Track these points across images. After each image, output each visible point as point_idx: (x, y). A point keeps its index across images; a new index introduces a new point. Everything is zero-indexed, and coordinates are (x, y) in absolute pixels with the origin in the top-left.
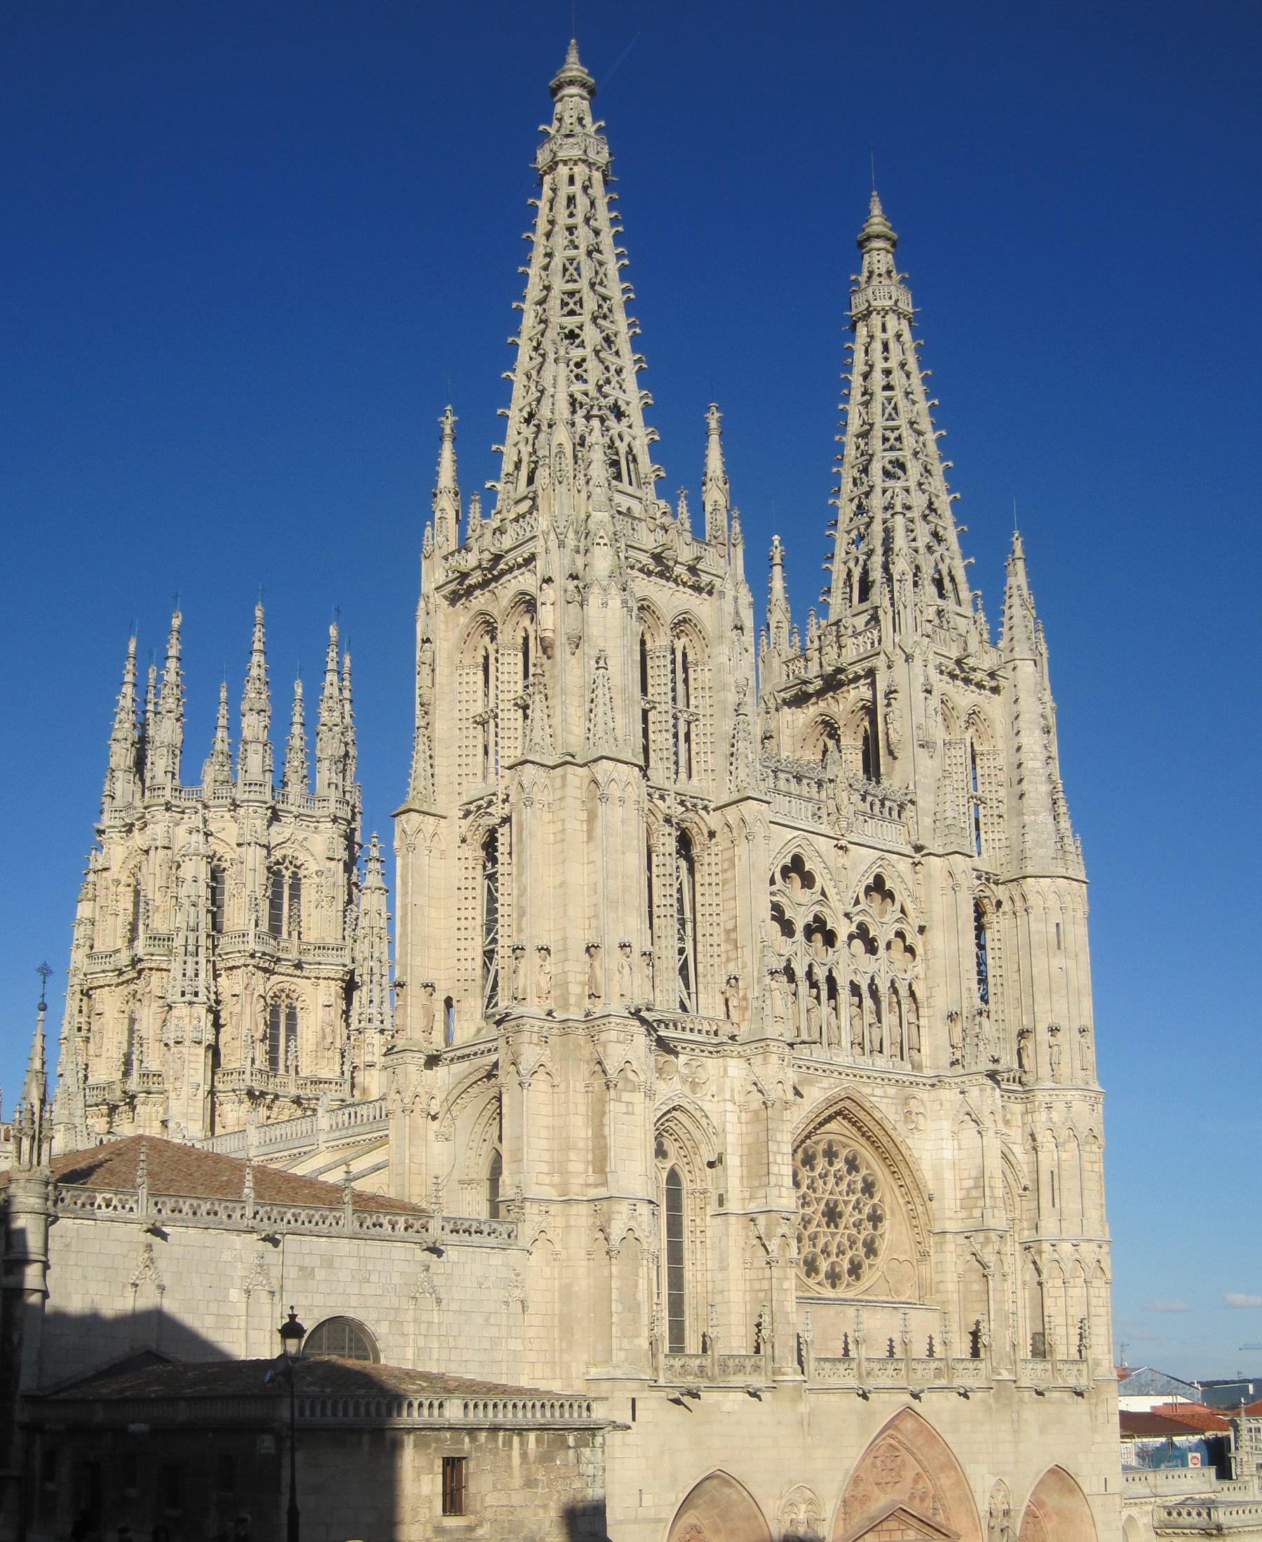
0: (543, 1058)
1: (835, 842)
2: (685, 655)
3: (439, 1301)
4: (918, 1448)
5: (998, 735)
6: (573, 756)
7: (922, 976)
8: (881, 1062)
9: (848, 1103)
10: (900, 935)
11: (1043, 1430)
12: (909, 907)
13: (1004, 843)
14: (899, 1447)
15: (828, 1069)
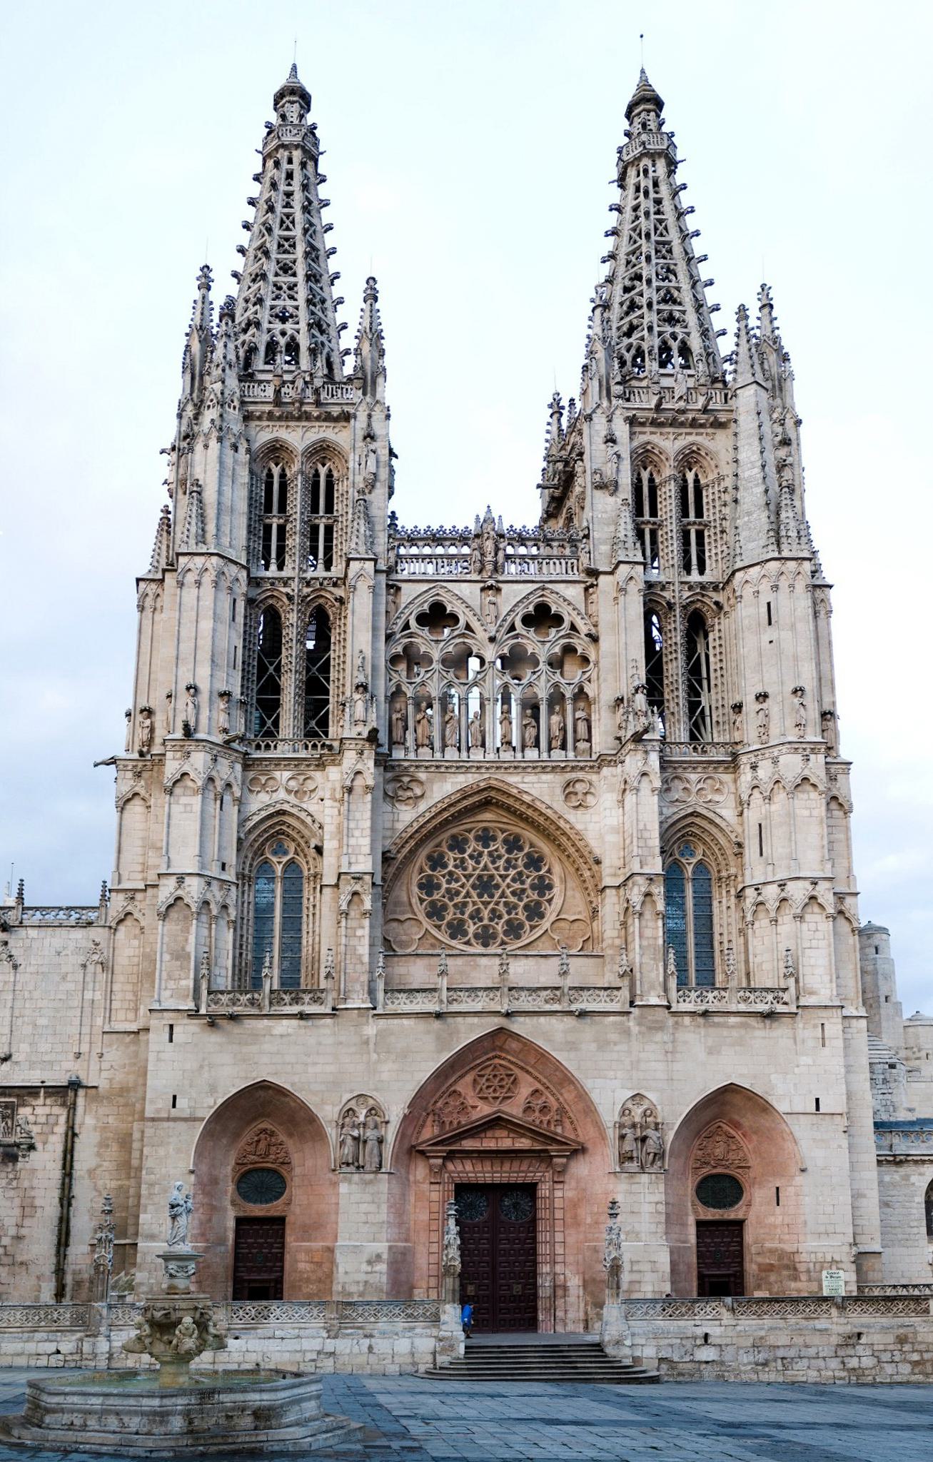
0: (137, 789)
1: (482, 585)
2: (329, 474)
3: (15, 967)
4: (532, 1067)
5: (723, 464)
6: (172, 565)
7: (594, 677)
8: (532, 754)
9: (493, 794)
10: (569, 650)
11: (711, 1051)
12: (580, 624)
13: (724, 554)
14: (512, 1067)
15: (461, 768)
